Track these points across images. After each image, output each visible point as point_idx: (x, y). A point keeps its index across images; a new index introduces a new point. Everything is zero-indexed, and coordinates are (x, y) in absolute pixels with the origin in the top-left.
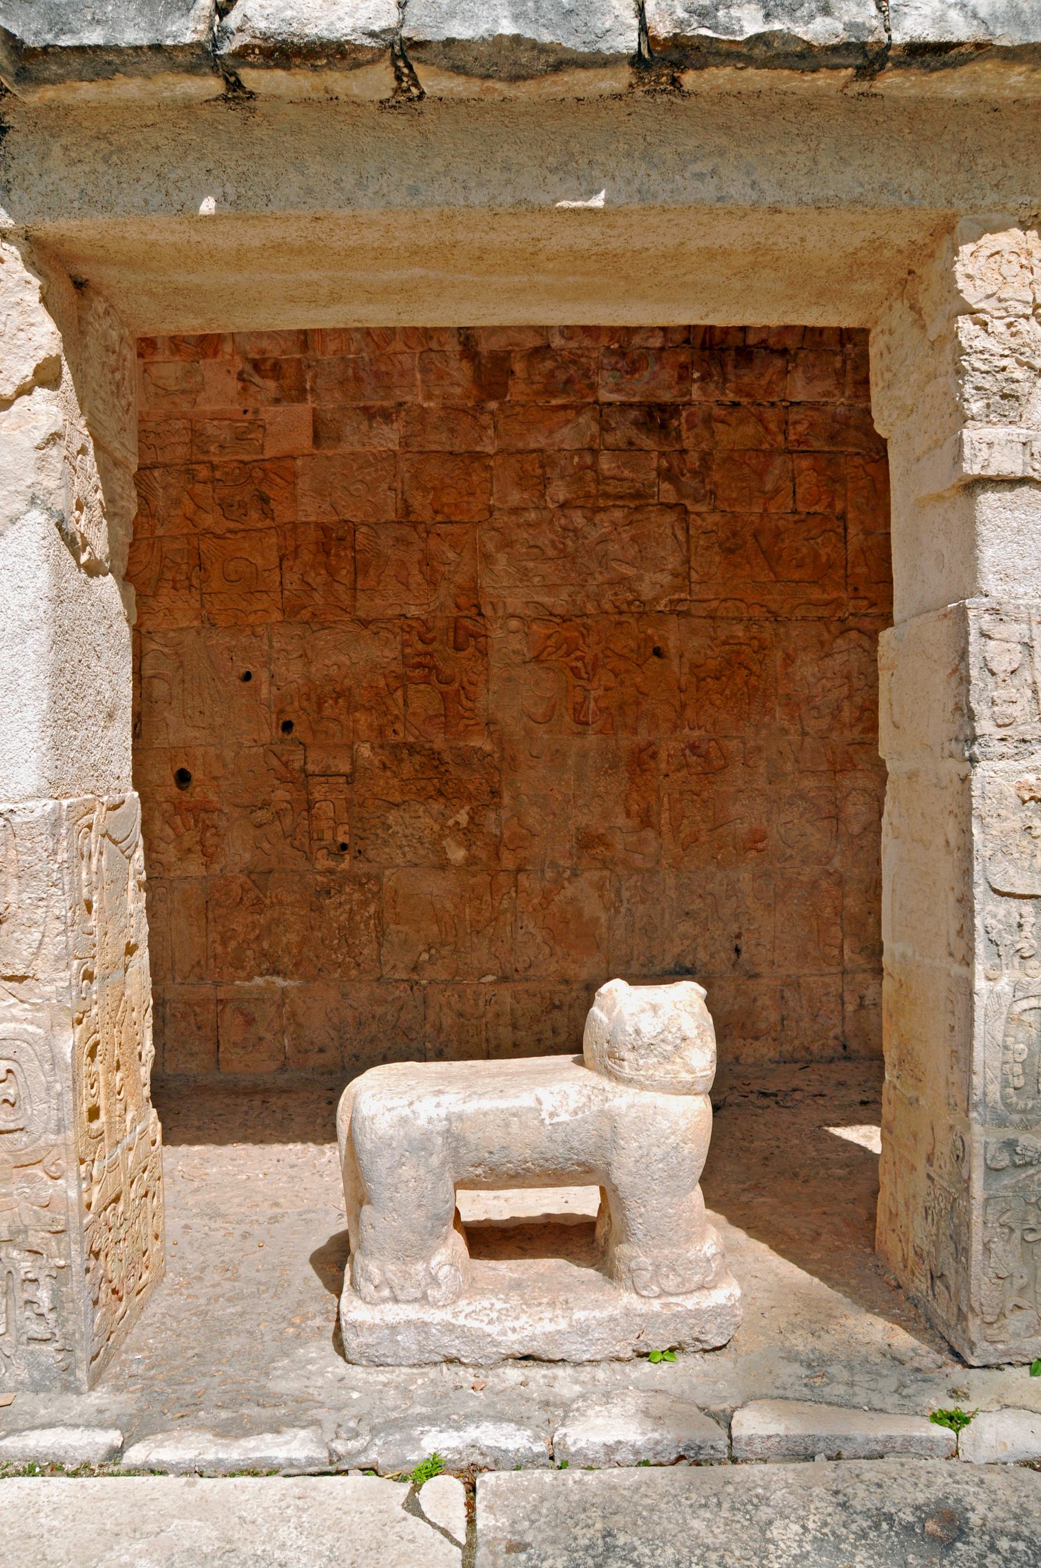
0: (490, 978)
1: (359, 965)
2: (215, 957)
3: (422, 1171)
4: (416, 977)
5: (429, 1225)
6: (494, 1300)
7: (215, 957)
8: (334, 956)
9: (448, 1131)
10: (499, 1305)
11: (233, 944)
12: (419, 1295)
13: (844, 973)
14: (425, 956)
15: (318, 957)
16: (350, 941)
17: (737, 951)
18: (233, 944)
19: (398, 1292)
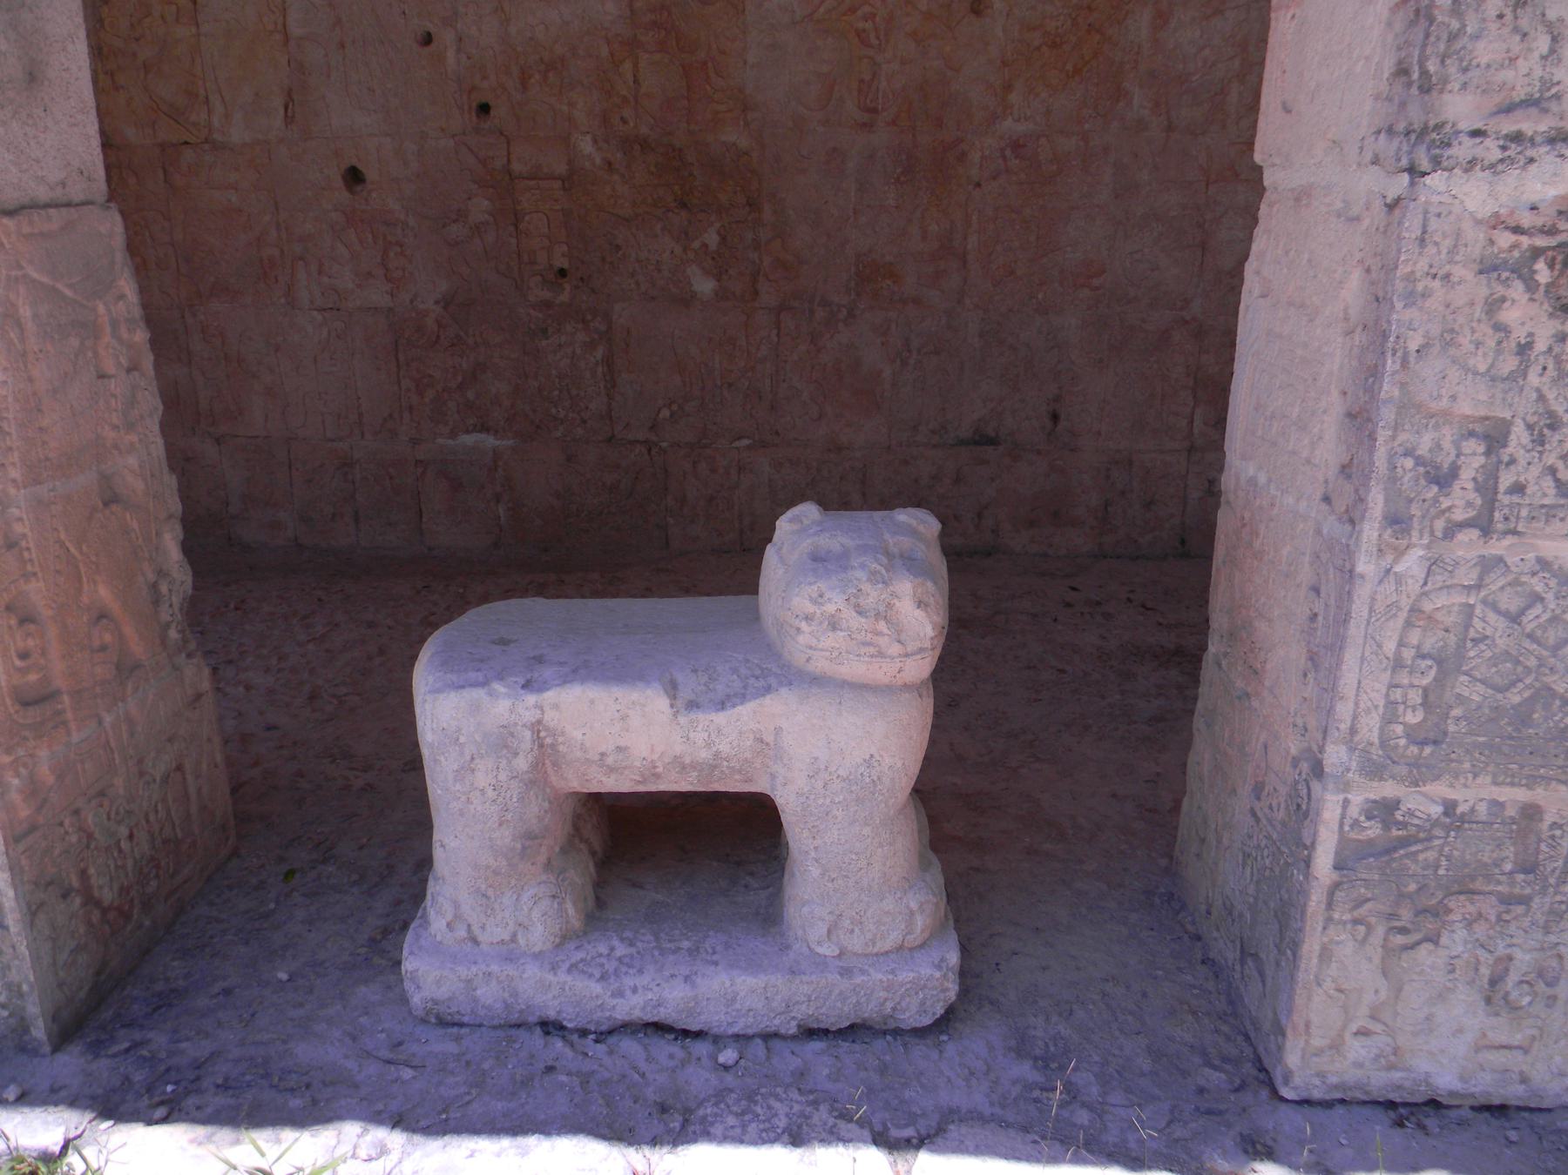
0: (746, 442)
1: (584, 422)
2: (411, 408)
3: (503, 776)
4: (654, 438)
5: (519, 846)
6: (616, 943)
7: (411, 408)
8: (554, 411)
9: (539, 722)
10: (621, 950)
11: (430, 394)
12: (507, 937)
13: (1191, 450)
14: (665, 413)
15: (534, 411)
16: (574, 392)
17: (1055, 417)
18: (430, 394)
19: (476, 930)
